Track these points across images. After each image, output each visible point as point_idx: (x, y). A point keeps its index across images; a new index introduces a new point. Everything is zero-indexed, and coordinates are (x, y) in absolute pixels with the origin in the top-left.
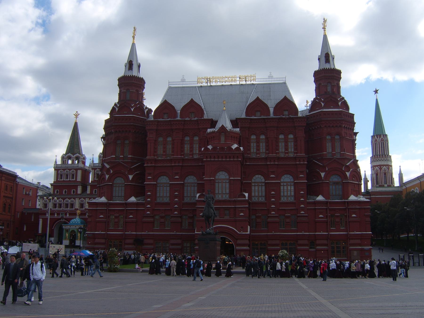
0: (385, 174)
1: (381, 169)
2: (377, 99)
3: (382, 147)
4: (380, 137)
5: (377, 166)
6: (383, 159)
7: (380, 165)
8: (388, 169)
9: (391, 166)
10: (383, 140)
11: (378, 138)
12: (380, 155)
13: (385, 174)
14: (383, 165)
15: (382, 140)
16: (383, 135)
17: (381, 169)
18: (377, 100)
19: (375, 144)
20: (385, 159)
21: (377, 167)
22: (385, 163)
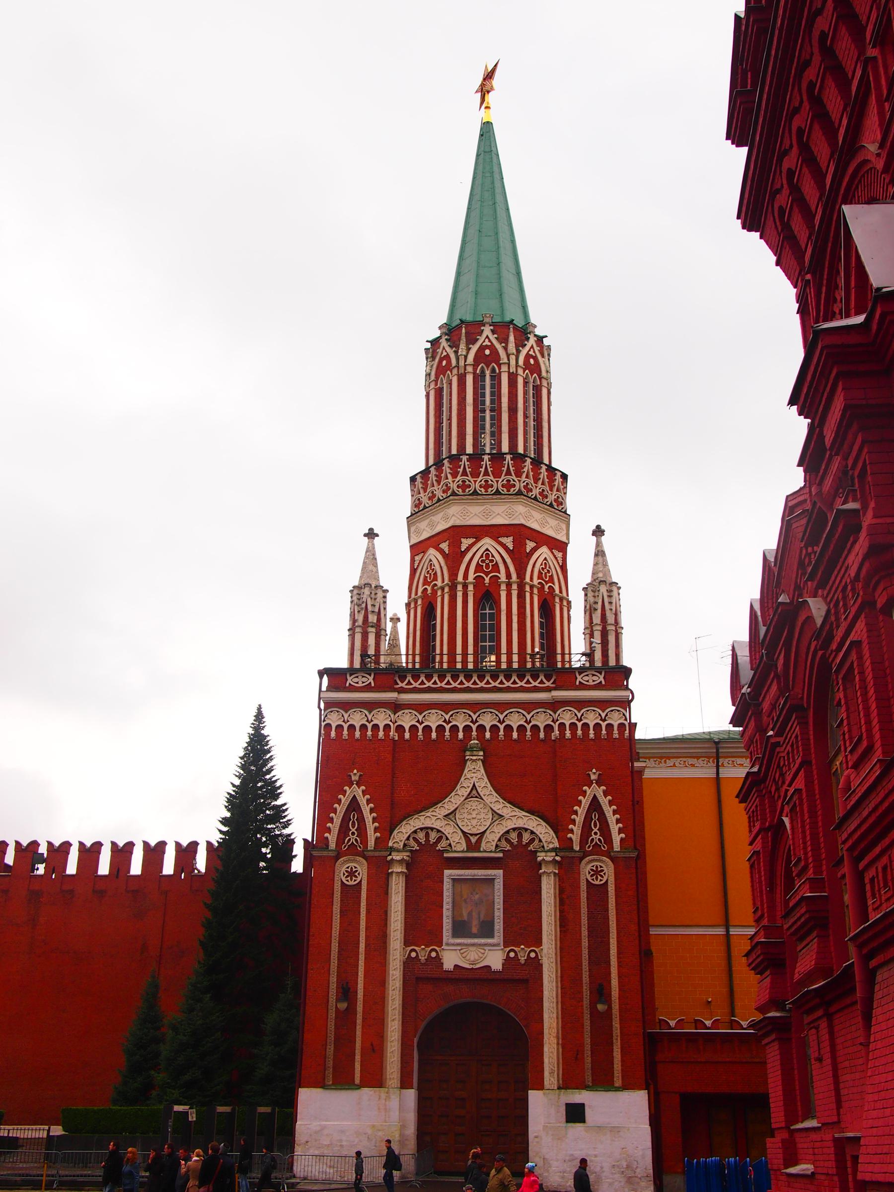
0: (487, 596)
1: (454, 559)
2: (487, 131)
3: (478, 409)
4: (471, 341)
5: (433, 541)
6: (476, 484)
7: (456, 533)
8: (520, 558)
9: (560, 546)
10: (495, 357)
11: (455, 345)
13: (487, 596)
14: (478, 532)
15: (488, 358)
16: (502, 328)
17: (454, 559)
18: (487, 131)
19: (439, 393)
20: (498, 484)
21: (432, 552)
22: (500, 513)
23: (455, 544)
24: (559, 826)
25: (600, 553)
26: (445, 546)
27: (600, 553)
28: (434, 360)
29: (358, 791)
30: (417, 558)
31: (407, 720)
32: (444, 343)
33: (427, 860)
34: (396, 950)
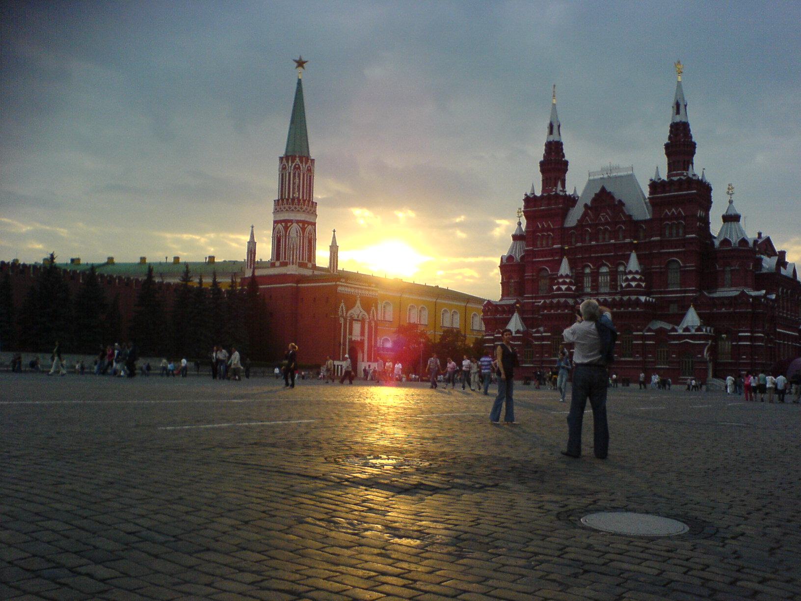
1: (303, 229)
2: (299, 83)
5: (298, 222)
11: (302, 162)
12: (304, 201)
14: (309, 223)
17: (303, 229)
19: (294, 174)
23: (303, 225)
24: (369, 314)
25: (334, 237)
26: (301, 225)
27: (334, 237)
28: (292, 162)
29: (342, 304)
30: (289, 224)
31: (349, 290)
32: (297, 159)
33: (352, 320)
34: (348, 336)
